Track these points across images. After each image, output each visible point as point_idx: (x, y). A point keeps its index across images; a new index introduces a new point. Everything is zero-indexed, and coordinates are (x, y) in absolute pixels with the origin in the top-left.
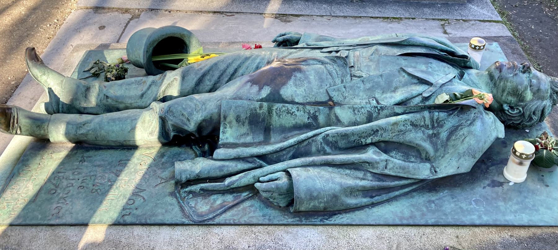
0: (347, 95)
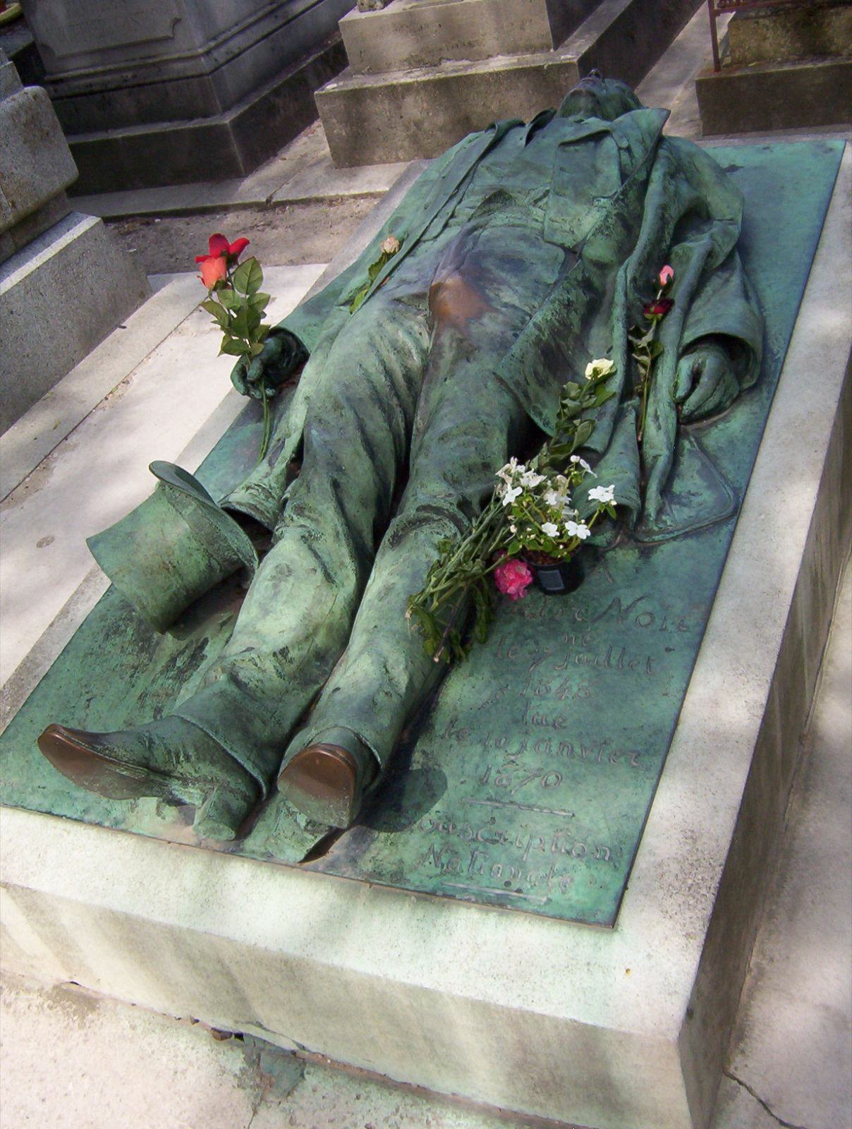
0: (568, 227)
